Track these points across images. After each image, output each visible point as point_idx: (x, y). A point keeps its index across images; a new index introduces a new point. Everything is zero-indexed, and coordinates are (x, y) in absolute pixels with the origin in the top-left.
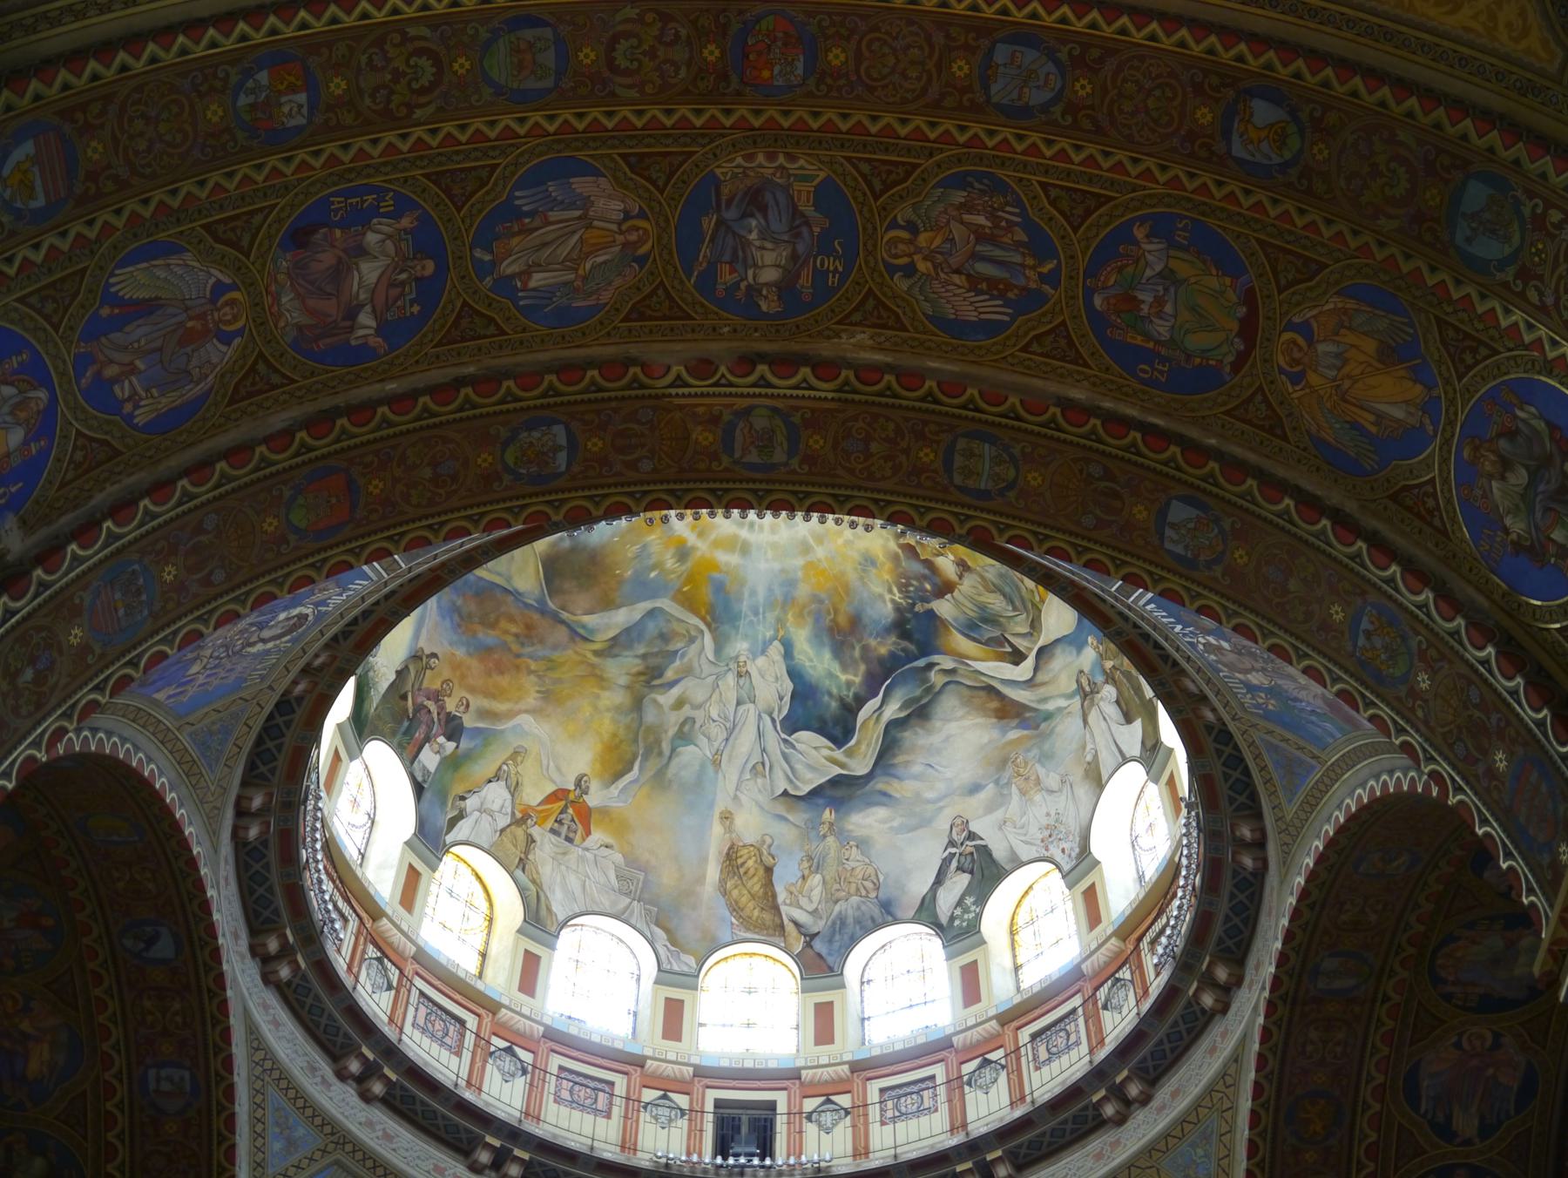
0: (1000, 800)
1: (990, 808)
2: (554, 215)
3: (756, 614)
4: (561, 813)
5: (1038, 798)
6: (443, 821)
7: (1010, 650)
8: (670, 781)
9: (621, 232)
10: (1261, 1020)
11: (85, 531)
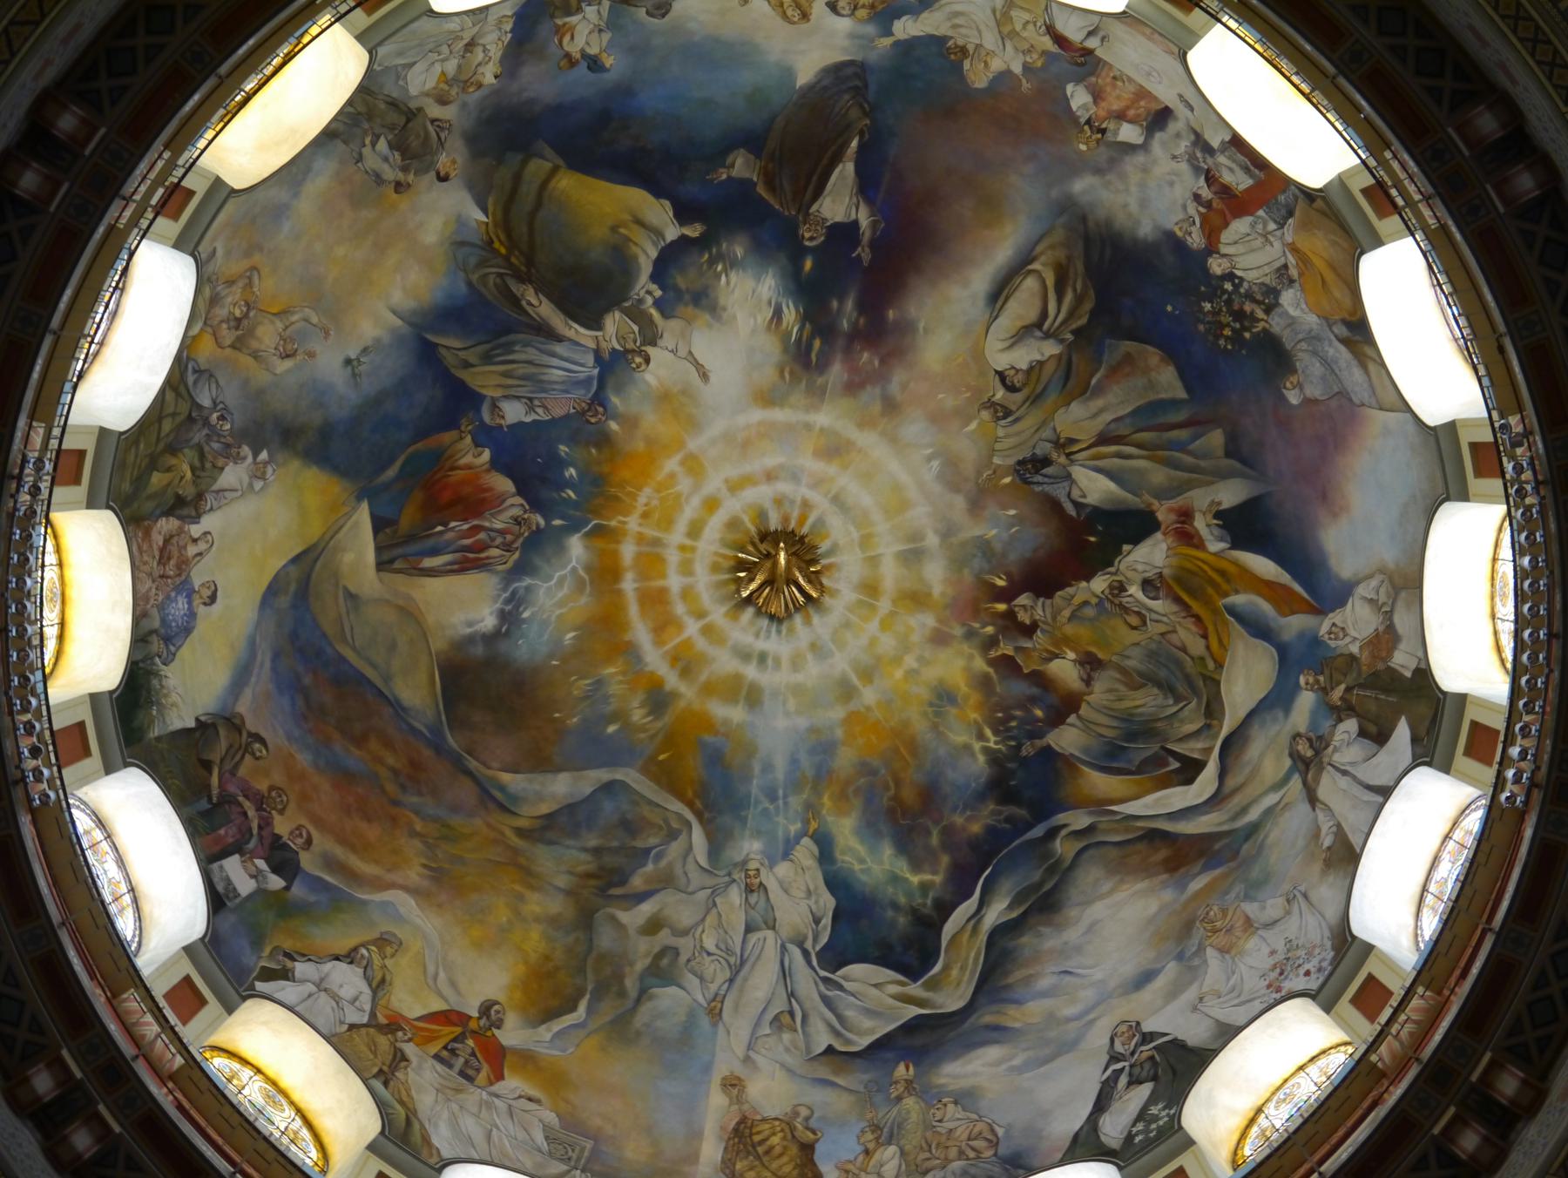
0: (1190, 964)
1: (1173, 993)
3: (773, 798)
4: (454, 1040)
5: (1252, 943)
7: (1175, 765)
8: (638, 1034)
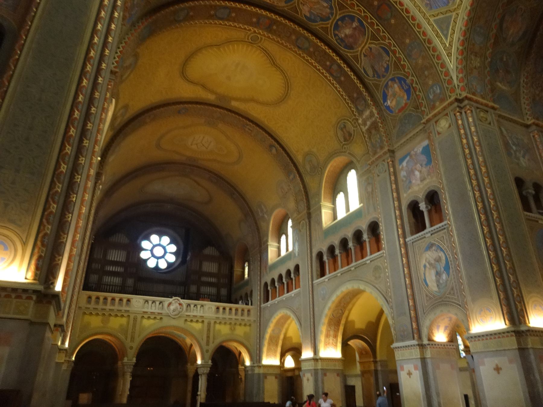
9: (306, 2)
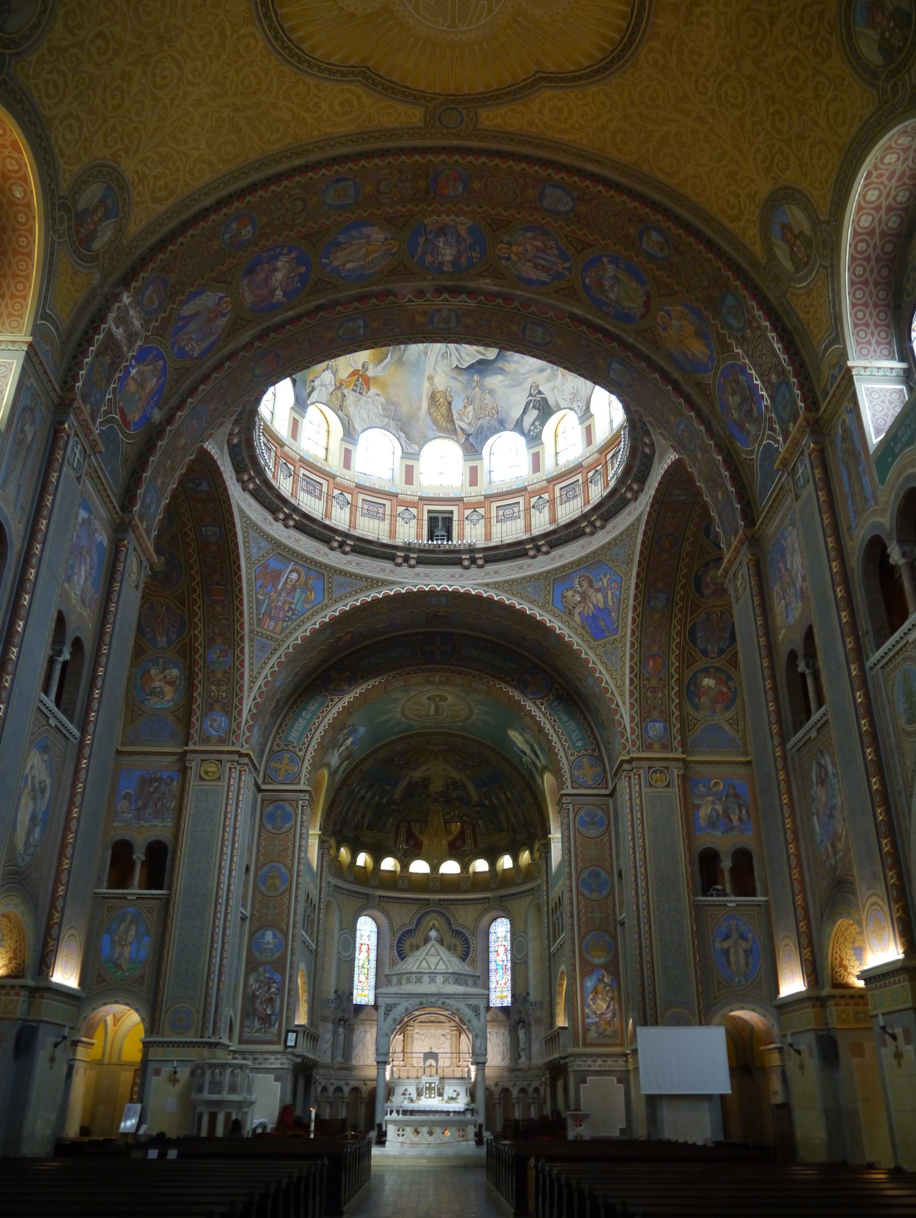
1: (549, 380)
2: (354, 242)
6: (306, 394)
10: (648, 509)
11: (180, 405)
